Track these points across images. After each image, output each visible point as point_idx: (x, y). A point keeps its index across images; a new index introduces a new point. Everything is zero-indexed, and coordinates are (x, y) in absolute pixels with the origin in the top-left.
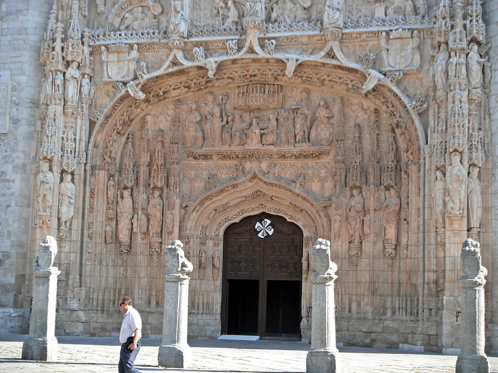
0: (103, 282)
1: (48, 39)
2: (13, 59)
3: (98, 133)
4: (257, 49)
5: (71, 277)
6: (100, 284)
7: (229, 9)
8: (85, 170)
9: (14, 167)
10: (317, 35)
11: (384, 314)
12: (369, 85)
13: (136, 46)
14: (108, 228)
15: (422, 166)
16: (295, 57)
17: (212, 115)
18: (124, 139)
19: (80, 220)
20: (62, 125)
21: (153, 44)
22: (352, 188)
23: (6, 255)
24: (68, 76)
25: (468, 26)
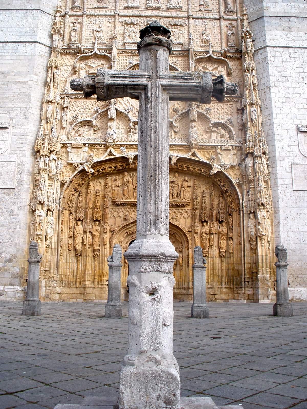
0: (68, 271)
1: (40, 138)
2: (18, 149)
3: (66, 190)
5: (52, 269)
6: (66, 273)
7: (135, 129)
8: (59, 210)
9: (18, 207)
10: (185, 145)
11: (221, 285)
12: (214, 171)
13: (87, 145)
14: (70, 242)
15: (241, 212)
16: (176, 155)
17: (128, 182)
18: (78, 194)
19: (57, 237)
20: (47, 185)
21: (97, 144)
22: (202, 222)
23: (14, 256)
24: (51, 158)
25: (261, 146)
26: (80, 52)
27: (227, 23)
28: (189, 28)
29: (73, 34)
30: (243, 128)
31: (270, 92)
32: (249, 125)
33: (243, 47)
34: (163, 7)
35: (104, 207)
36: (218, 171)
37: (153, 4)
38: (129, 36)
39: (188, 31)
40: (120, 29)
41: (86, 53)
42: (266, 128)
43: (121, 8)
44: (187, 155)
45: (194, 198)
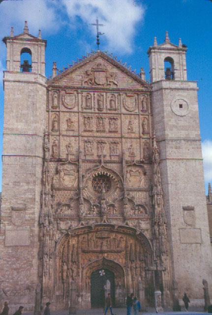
4: (106, 222)
7: (94, 209)
12: (138, 233)
26: (61, 161)
27: (144, 140)
28: (122, 144)
29: (55, 148)
30: (153, 207)
31: (168, 187)
32: (156, 207)
33: (153, 159)
34: (107, 130)
35: (78, 254)
36: (140, 233)
37: (102, 129)
38: (88, 150)
39: (122, 147)
40: (82, 144)
41: (63, 161)
42: (165, 207)
43: (82, 130)
44: (124, 224)
45: (126, 247)
